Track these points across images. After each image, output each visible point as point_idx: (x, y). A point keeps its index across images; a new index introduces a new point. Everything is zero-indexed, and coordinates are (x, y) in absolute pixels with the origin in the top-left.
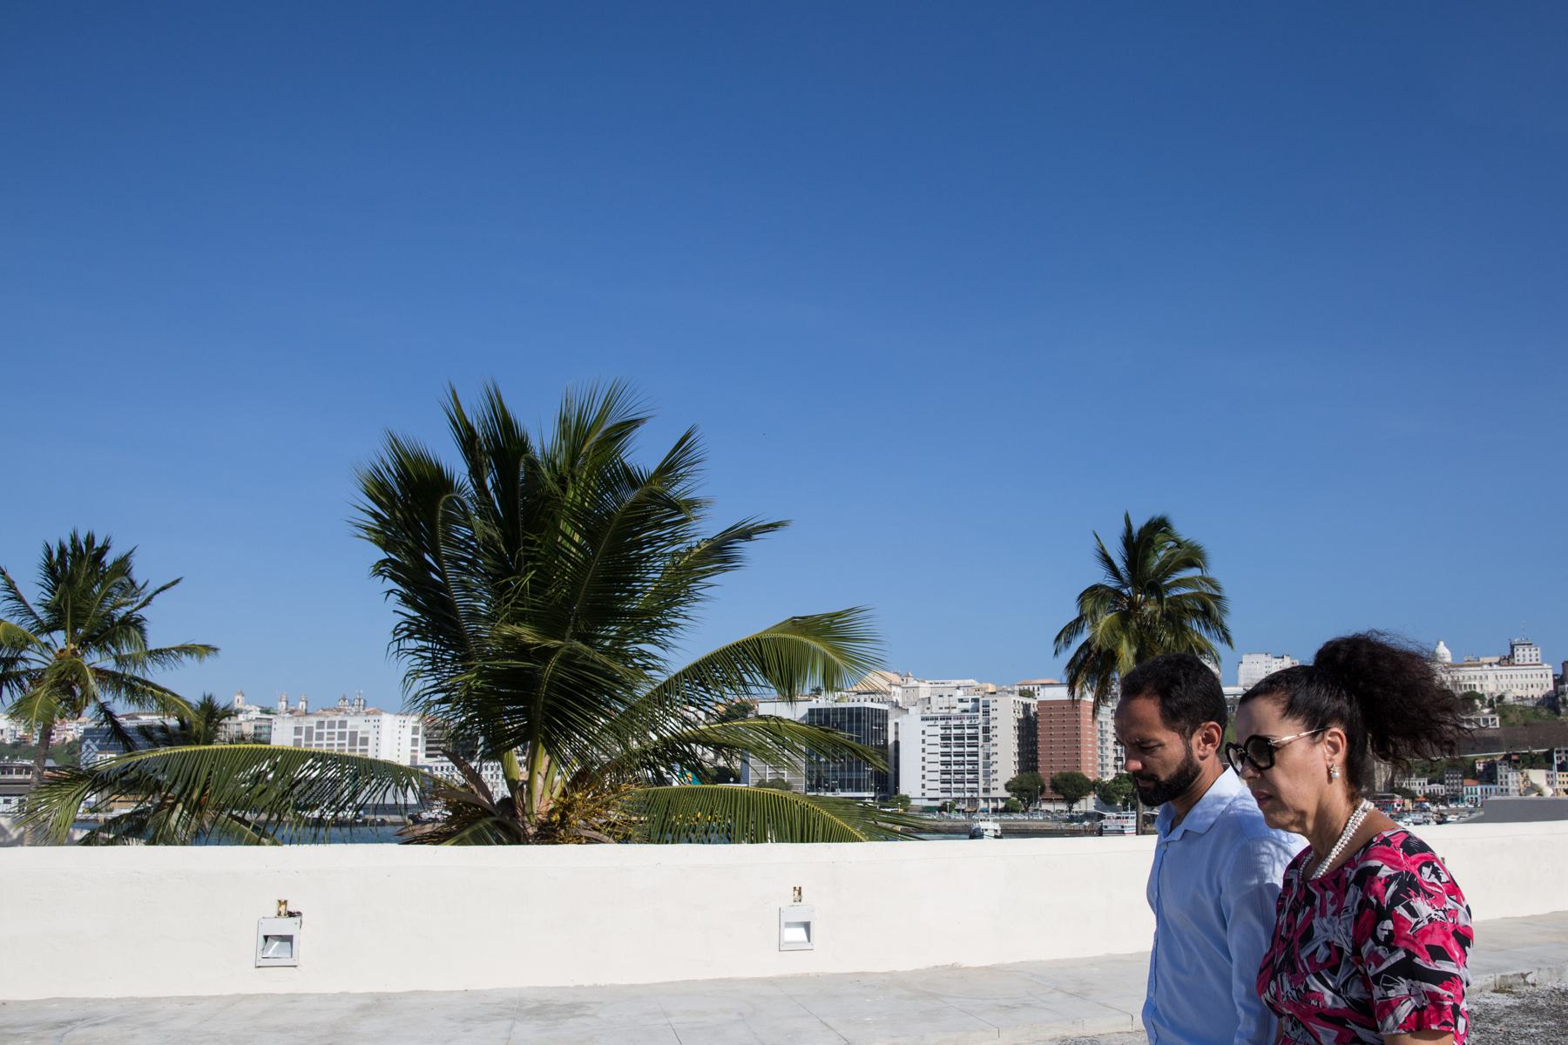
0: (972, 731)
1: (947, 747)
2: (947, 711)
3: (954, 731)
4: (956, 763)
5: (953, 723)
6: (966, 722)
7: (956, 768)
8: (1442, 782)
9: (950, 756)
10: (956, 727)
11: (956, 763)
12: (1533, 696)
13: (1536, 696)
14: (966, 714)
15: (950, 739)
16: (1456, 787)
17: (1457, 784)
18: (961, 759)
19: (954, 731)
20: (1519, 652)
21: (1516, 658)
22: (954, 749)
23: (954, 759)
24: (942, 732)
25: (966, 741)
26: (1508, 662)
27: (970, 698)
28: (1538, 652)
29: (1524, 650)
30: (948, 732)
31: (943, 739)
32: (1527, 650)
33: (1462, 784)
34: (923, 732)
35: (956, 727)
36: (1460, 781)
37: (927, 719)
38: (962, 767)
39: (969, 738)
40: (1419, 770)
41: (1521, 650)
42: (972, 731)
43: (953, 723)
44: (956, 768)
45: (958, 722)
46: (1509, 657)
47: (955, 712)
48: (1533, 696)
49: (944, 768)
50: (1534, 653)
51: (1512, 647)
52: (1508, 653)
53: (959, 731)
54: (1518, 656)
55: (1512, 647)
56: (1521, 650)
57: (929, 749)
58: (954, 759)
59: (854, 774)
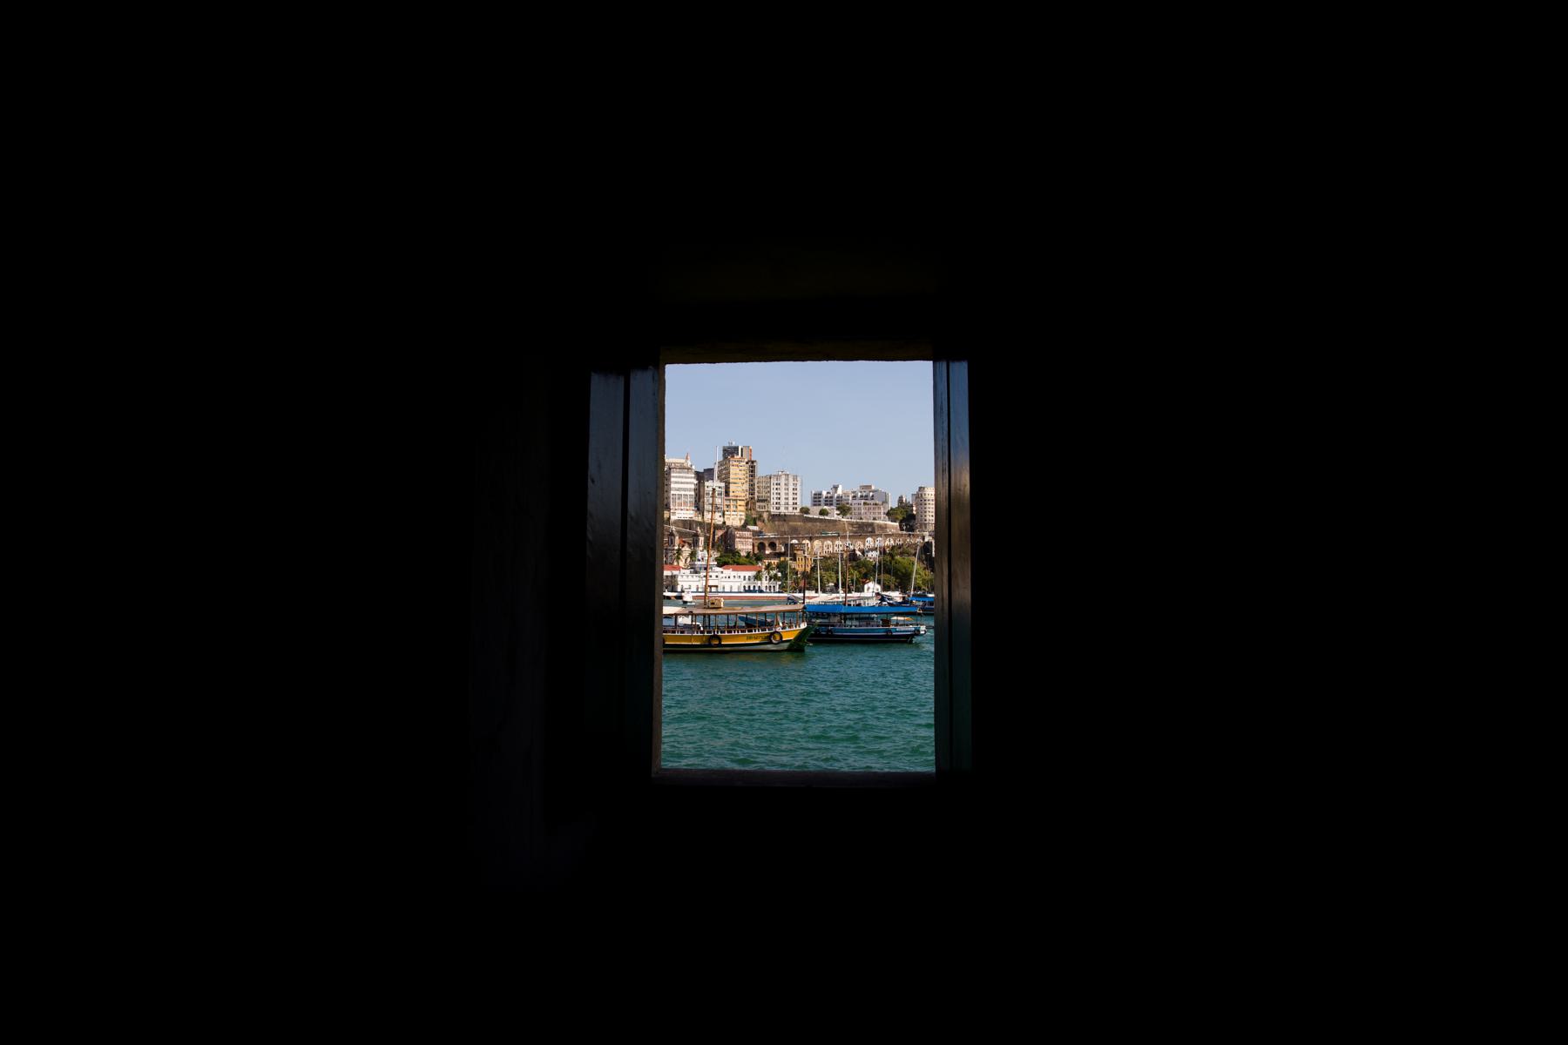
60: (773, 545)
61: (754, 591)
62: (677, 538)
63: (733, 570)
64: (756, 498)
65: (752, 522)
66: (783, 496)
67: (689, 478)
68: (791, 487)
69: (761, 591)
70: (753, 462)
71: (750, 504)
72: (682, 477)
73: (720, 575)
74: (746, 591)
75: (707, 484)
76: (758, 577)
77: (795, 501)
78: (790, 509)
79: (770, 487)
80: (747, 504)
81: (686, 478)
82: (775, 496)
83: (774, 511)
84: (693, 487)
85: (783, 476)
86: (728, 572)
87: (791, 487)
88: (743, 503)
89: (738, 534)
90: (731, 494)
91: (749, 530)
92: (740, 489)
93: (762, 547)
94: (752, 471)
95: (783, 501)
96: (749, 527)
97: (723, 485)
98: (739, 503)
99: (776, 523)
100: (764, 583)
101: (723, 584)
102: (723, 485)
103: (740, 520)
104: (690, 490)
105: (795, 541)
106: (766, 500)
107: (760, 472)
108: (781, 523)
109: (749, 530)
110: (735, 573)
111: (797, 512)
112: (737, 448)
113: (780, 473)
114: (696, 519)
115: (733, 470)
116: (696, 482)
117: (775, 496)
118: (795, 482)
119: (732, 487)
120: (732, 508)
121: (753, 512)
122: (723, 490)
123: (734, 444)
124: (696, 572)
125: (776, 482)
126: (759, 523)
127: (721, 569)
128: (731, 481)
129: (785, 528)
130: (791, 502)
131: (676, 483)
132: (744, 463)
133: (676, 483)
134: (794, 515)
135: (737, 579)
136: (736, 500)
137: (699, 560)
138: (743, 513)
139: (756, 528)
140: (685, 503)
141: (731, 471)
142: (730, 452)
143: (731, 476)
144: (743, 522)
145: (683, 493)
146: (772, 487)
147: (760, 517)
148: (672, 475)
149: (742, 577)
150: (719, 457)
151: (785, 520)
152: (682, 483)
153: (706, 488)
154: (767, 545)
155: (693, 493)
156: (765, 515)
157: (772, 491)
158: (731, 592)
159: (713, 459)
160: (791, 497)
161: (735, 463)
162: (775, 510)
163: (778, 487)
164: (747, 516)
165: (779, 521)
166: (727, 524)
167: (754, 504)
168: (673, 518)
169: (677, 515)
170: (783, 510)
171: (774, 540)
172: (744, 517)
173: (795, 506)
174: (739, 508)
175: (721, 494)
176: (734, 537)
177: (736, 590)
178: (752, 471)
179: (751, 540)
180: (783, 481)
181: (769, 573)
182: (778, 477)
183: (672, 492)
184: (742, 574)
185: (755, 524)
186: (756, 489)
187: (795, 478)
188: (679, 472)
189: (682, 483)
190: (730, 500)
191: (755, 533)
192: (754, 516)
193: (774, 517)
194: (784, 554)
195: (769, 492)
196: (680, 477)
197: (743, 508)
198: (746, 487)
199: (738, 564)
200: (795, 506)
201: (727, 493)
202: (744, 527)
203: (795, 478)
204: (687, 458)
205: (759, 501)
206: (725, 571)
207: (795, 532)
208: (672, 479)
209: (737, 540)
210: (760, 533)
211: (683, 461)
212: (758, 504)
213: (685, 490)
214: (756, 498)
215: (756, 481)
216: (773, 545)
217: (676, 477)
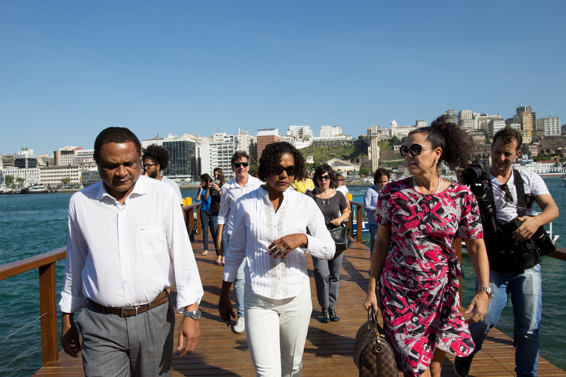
0: (230, 149)
1: (220, 156)
2: (220, 141)
3: (223, 149)
4: (224, 162)
5: (222, 146)
6: (228, 146)
7: (225, 164)
8: (397, 169)
9: (222, 159)
10: (224, 148)
11: (224, 162)
14: (228, 142)
15: (221, 152)
16: (402, 171)
17: (402, 169)
18: (226, 160)
19: (223, 149)
22: (224, 157)
23: (223, 160)
24: (219, 150)
25: (228, 153)
27: (229, 136)
28: (426, 123)
30: (221, 150)
31: (218, 153)
32: (422, 122)
33: (404, 169)
34: (211, 150)
35: (224, 148)
36: (403, 168)
37: (212, 145)
38: (227, 164)
39: (229, 152)
40: (388, 165)
41: (420, 122)
42: (230, 149)
43: (222, 146)
44: (225, 164)
45: (225, 146)
47: (223, 142)
49: (219, 164)
50: (424, 124)
52: (415, 124)
53: (225, 149)
55: (417, 122)
56: (420, 122)
57: (213, 157)
58: (223, 160)
59: (183, 168)
60: (548, 151)
61: (554, 172)
63: (542, 163)
64: (537, 130)
65: (536, 141)
66: (551, 128)
67: (502, 123)
68: (555, 123)
69: (558, 172)
70: (534, 113)
71: (534, 132)
72: (499, 123)
73: (536, 166)
74: (551, 172)
76: (556, 166)
77: (558, 130)
78: (556, 133)
79: (544, 124)
80: (532, 133)
81: (501, 123)
82: (547, 128)
83: (546, 135)
85: (551, 119)
86: (540, 164)
87: (555, 123)
88: (530, 132)
89: (530, 147)
90: (524, 129)
91: (535, 145)
92: (528, 126)
93: (542, 152)
94: (534, 118)
95: (551, 130)
96: (534, 143)
97: (520, 125)
98: (528, 132)
99: (548, 140)
100: (560, 168)
101: (538, 169)
102: (520, 125)
103: (529, 140)
105: (560, 148)
106: (542, 130)
107: (537, 118)
108: (551, 140)
109: (535, 145)
110: (543, 164)
111: (560, 134)
112: (524, 107)
113: (549, 117)
115: (524, 118)
116: (506, 125)
117: (547, 128)
118: (558, 120)
119: (524, 126)
121: (535, 136)
122: (520, 127)
124: (523, 165)
125: (547, 121)
126: (539, 141)
127: (535, 163)
128: (524, 123)
129: (554, 142)
130: (556, 130)
131: (496, 126)
132: (530, 114)
133: (496, 126)
134: (558, 136)
135: (544, 167)
136: (527, 132)
137: (524, 159)
138: (531, 137)
139: (538, 144)
141: (524, 118)
142: (520, 110)
143: (524, 121)
144: (531, 141)
146: (545, 124)
147: (540, 138)
148: (494, 122)
149: (547, 166)
150: (515, 113)
151: (553, 139)
152: (499, 126)
154: (545, 151)
156: (542, 137)
157: (545, 126)
158: (542, 173)
159: (512, 114)
160: (555, 128)
161: (525, 114)
162: (547, 135)
163: (548, 123)
164: (533, 138)
165: (550, 139)
167: (536, 132)
170: (551, 134)
171: (549, 149)
172: (531, 139)
173: (558, 132)
174: (528, 135)
176: (528, 148)
177: (545, 172)
178: (534, 118)
179: (537, 149)
180: (551, 121)
181: (562, 163)
182: (548, 119)
183: (494, 130)
184: (547, 164)
185: (537, 142)
186: (536, 126)
187: (557, 118)
188: (498, 121)
189: (499, 126)
191: (538, 146)
192: (536, 138)
193: (546, 138)
194: (555, 155)
195: (544, 126)
196: (498, 123)
197: (530, 135)
198: (531, 125)
199: (543, 160)
200: (558, 132)
202: (532, 143)
203: (557, 118)
204: (499, 115)
205: (538, 131)
206: (538, 164)
207: (559, 144)
208: (494, 125)
210: (540, 146)
211: (497, 116)
212: (538, 132)
214: (537, 130)
215: (536, 122)
216: (548, 151)
217: (496, 123)
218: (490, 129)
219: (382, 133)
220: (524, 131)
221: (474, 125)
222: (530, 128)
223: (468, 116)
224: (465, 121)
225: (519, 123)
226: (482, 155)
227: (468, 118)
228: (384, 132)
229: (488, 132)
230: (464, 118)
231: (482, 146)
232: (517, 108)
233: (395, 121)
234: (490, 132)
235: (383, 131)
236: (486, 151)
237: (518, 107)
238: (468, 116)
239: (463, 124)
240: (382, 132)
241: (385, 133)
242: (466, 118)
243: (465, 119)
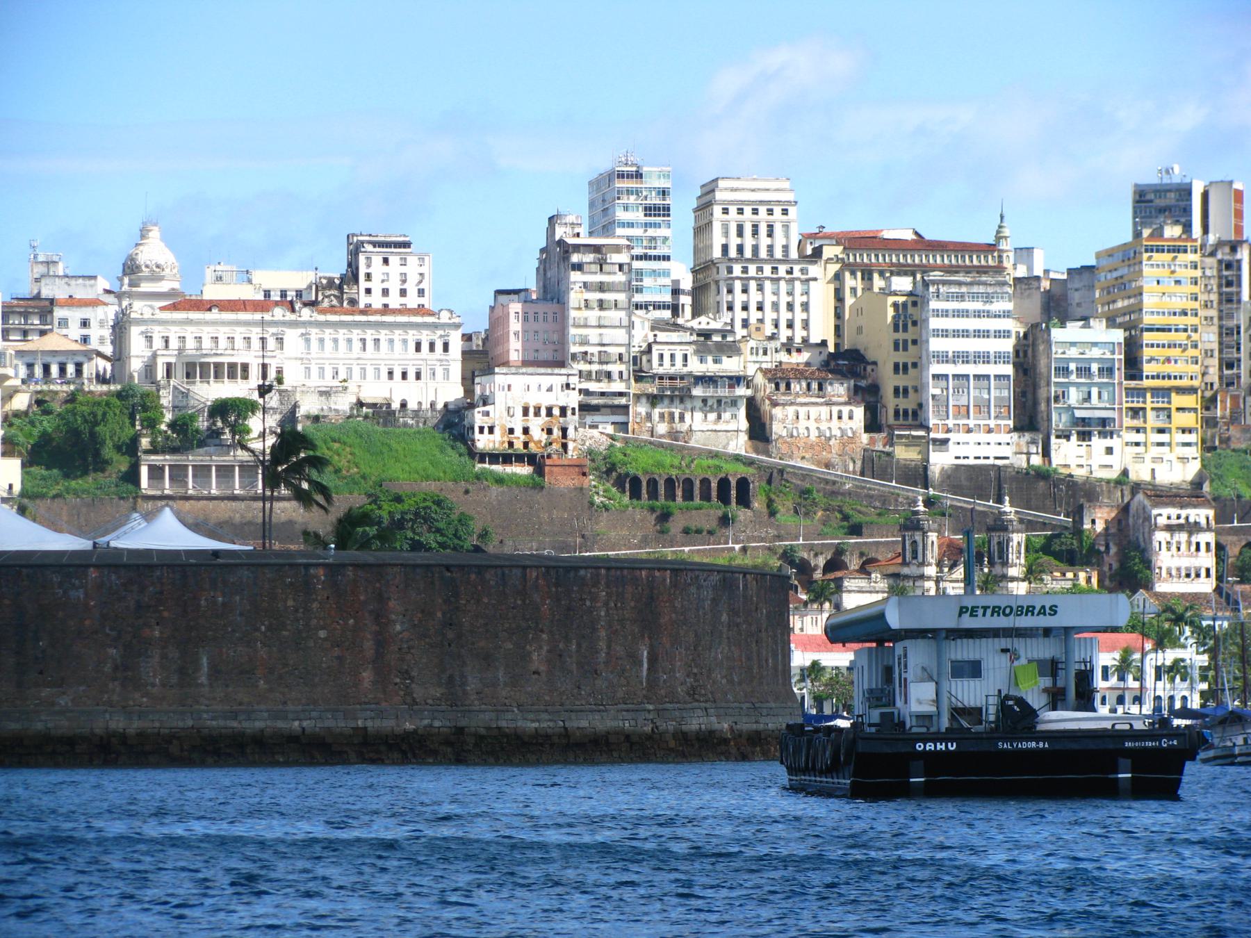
12: (404, 405)
13: (412, 405)
20: (372, 264)
21: (363, 284)
26: (341, 300)
29: (386, 261)
32: (394, 260)
41: (377, 260)
46: (342, 278)
48: (404, 405)
51: (355, 252)
52: (337, 269)
54: (368, 277)
62: (933, 536)
75: (1057, 334)
80: (1209, 403)
84: (1008, 345)
89: (1164, 514)
90: (1148, 369)
97: (1118, 335)
98: (1177, 400)
102: (1118, 335)
104: (999, 357)
112: (1185, 192)
114: (1021, 462)
120: (1152, 420)
123: (1177, 176)
128: (1148, 320)
131: (945, 333)
133: (945, 333)
140: (983, 407)
143: (1149, 301)
145: (970, 369)
153: (1057, 352)
155: (1008, 370)
166: (1133, 476)
168: (940, 461)
169: (953, 450)
175: (1110, 371)
179: (1209, 537)
190: (1141, 392)
197: (1189, 420)
198: (1209, 338)
201: (1133, 365)
208: (935, 323)
209: (1160, 536)
213: (983, 358)
218: (901, 357)
219: (64, 323)
220: (1146, 383)
221: (805, 307)
222: (1197, 369)
223: (763, 230)
224: (737, 270)
225: (1112, 323)
226: (821, 561)
227: (764, 241)
228: (75, 315)
229: (889, 381)
230: (734, 241)
231: (832, 489)
232: (1136, 185)
233: (168, 240)
234: (901, 380)
235: (71, 302)
236: (856, 530)
237: (1151, 178)
238: (763, 230)
239: (726, 298)
240: (59, 313)
241: (85, 323)
242: (749, 242)
243: (740, 249)
